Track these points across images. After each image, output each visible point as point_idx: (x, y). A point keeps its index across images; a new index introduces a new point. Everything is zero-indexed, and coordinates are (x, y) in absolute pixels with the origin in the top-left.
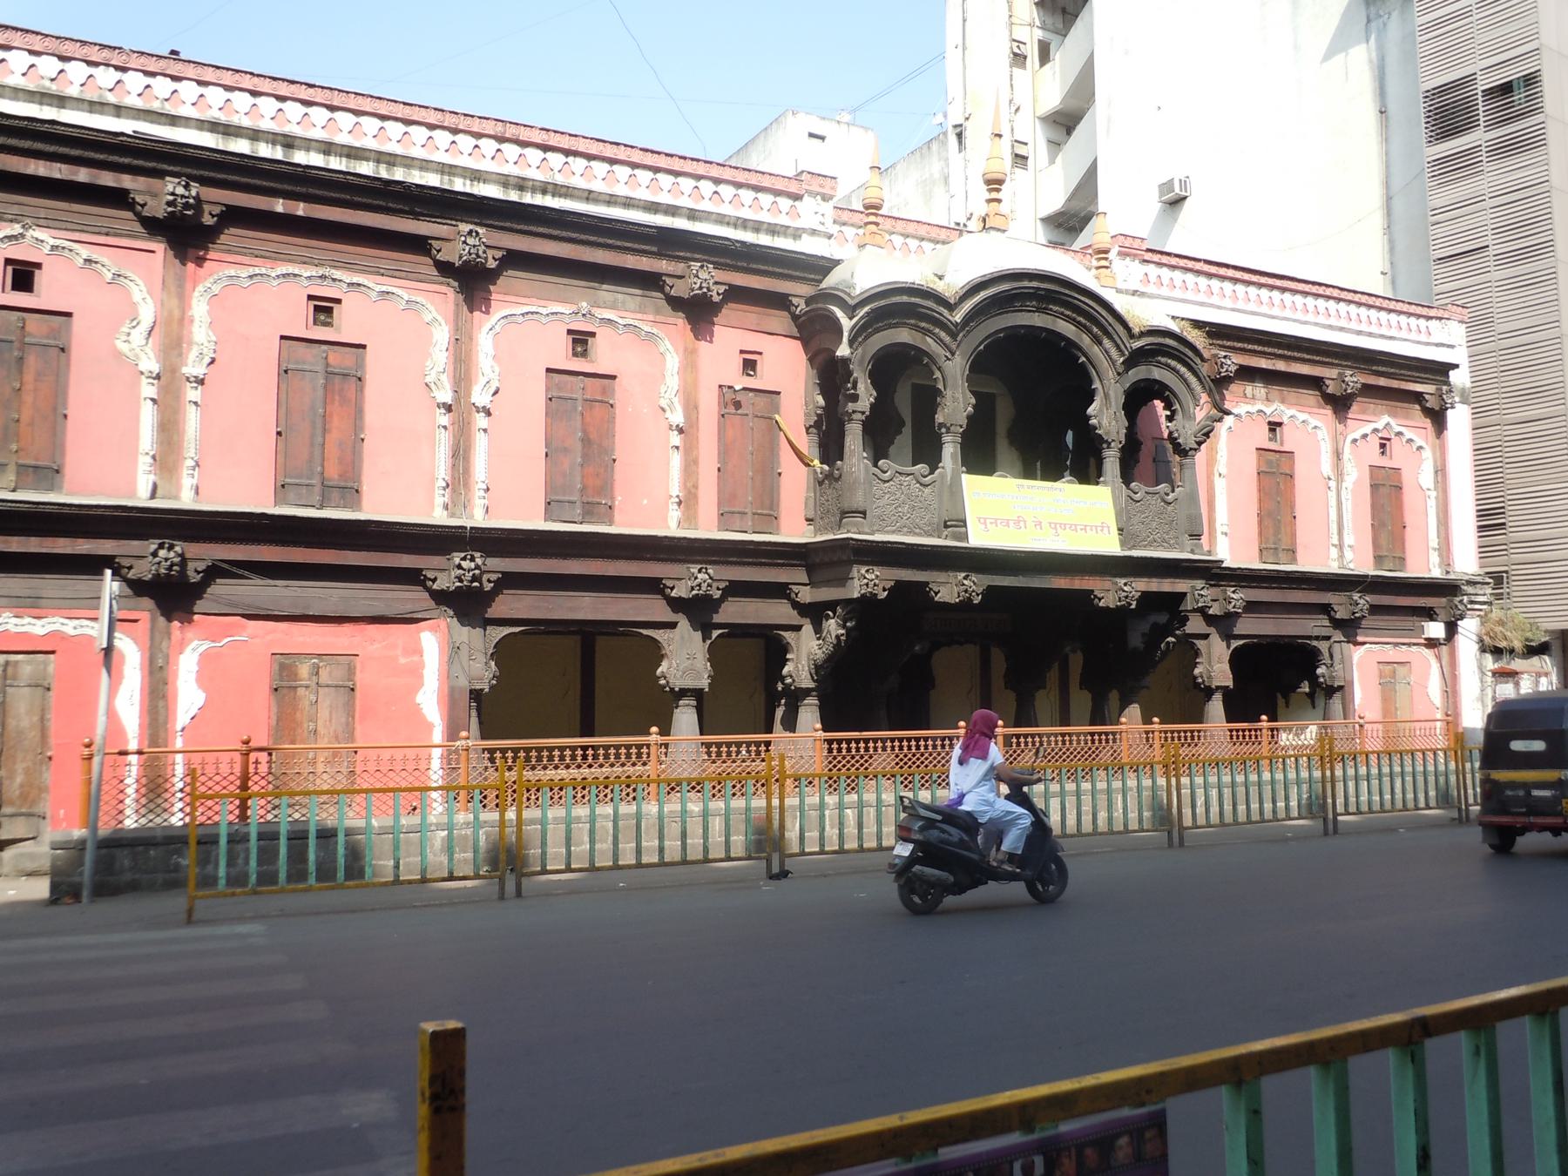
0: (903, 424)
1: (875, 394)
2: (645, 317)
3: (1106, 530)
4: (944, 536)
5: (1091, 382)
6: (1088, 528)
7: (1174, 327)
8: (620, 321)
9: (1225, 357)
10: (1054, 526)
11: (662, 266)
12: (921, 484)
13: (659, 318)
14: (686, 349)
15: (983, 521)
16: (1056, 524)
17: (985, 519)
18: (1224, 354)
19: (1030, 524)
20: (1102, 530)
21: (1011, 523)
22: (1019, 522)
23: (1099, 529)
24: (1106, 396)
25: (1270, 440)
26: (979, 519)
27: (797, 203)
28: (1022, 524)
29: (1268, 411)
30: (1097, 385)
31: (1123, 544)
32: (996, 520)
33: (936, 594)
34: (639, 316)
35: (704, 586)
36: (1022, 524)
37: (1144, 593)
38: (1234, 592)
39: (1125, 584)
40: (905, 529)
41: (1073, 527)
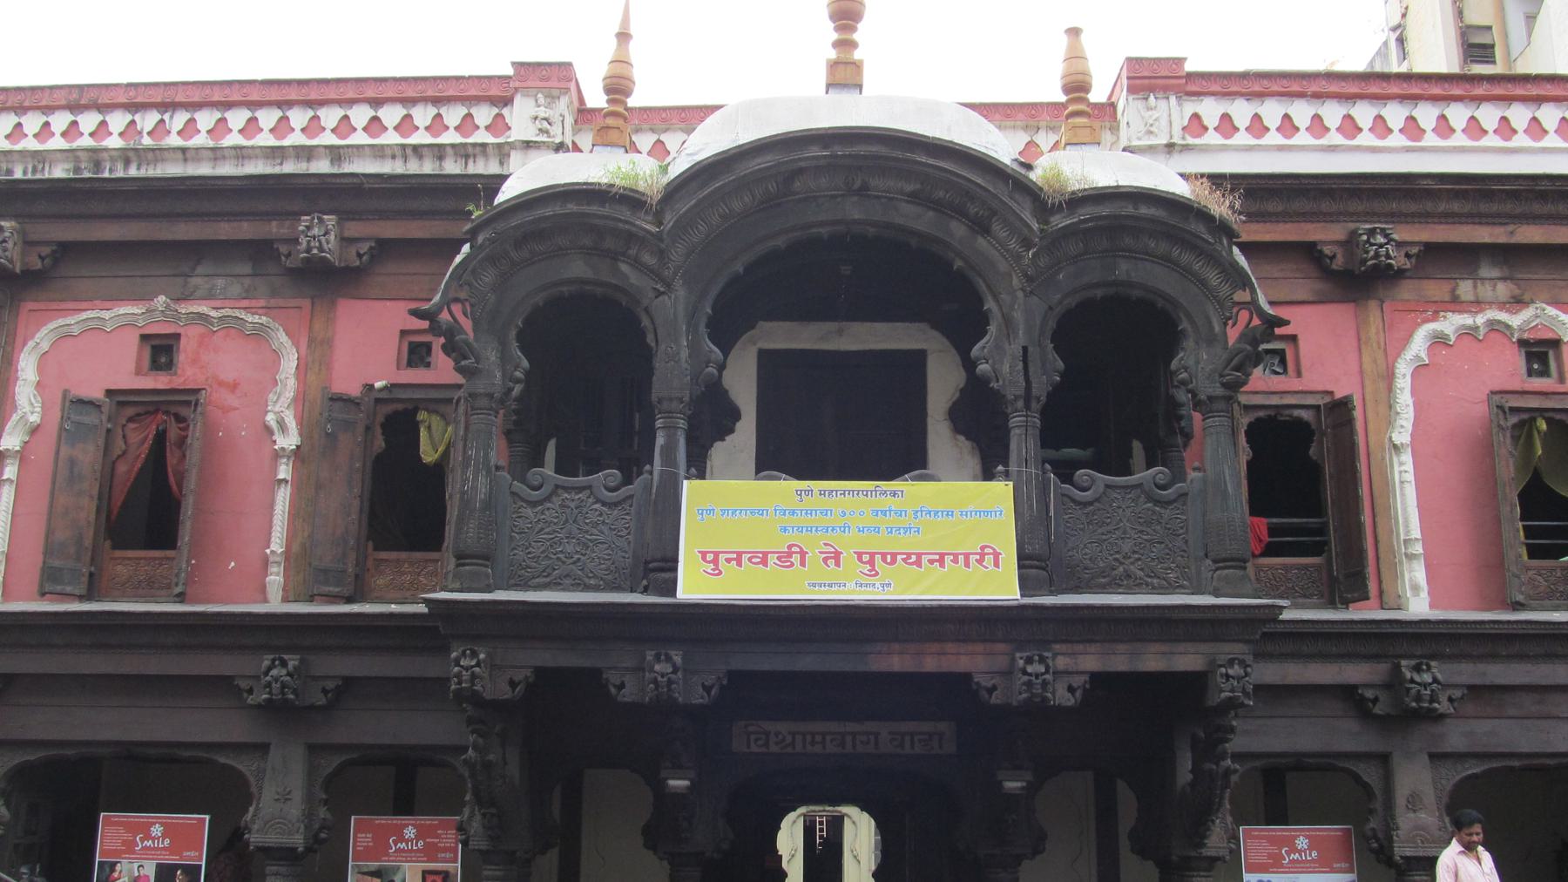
0: (735, 415)
1: (525, 364)
2: (254, 303)
3: (989, 559)
4: (641, 589)
5: (980, 301)
6: (948, 559)
7: (1182, 189)
8: (213, 314)
9: (1372, 232)
10: (869, 559)
11: (274, 229)
12: (604, 504)
13: (273, 302)
14: (311, 341)
15: (713, 559)
16: (872, 555)
17: (716, 554)
18: (1368, 226)
19: (814, 556)
20: (980, 561)
21: (772, 559)
22: (790, 554)
23: (973, 558)
24: (1008, 322)
25: (1530, 373)
26: (704, 554)
27: (505, 111)
28: (796, 559)
29: (1516, 320)
30: (990, 304)
31: (1025, 585)
32: (740, 554)
33: (621, 686)
34: (245, 303)
35: (276, 686)
36: (796, 559)
37: (1095, 677)
38: (1417, 669)
39: (1029, 661)
40: (568, 581)
41: (914, 558)
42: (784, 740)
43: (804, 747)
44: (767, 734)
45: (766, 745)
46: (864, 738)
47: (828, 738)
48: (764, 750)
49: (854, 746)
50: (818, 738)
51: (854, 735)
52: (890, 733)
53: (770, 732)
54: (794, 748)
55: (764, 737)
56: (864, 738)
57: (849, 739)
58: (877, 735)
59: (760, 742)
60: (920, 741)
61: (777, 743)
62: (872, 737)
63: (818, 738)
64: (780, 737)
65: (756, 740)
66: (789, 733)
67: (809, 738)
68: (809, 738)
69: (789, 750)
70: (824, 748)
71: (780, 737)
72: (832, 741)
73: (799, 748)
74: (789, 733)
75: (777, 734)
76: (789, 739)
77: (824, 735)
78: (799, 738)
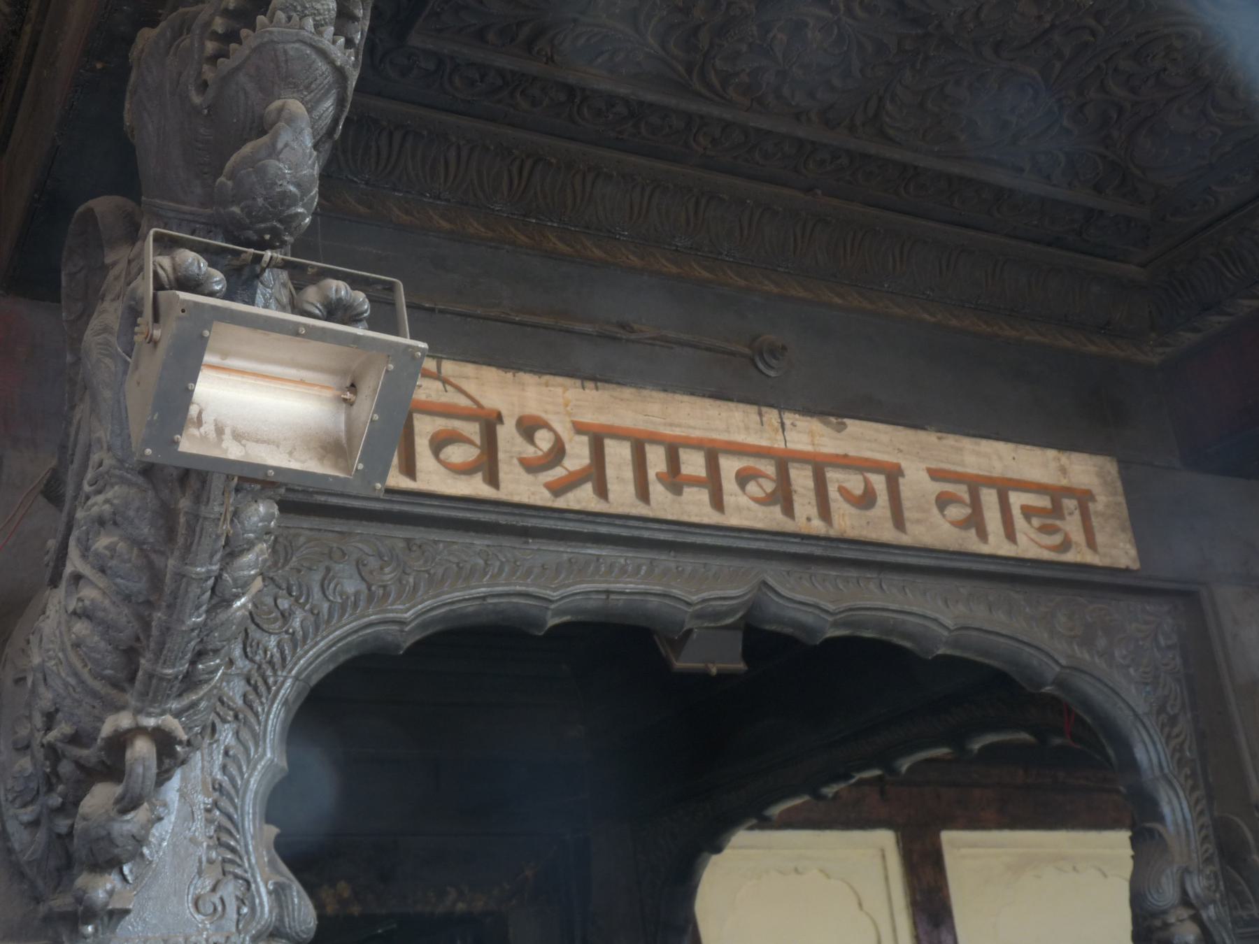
42: (558, 452)
43: (643, 493)
44: (490, 423)
45: (489, 466)
46: (855, 484)
47: (730, 466)
48: (475, 487)
49: (825, 511)
50: (693, 464)
51: (819, 466)
52: (936, 475)
53: (499, 418)
54: (602, 491)
55: (472, 430)
56: (855, 484)
57: (802, 479)
58: (893, 475)
59: (456, 454)
60: (1028, 512)
61: (532, 467)
62: (879, 482)
63: (693, 464)
64: (544, 441)
65: (439, 443)
66: (579, 429)
67: (656, 459)
68: (656, 459)
69: (583, 498)
70: (717, 502)
71: (544, 441)
72: (743, 479)
73: (622, 497)
74: (579, 429)
75: (528, 427)
76: (578, 456)
77: (712, 455)
78: (618, 454)
